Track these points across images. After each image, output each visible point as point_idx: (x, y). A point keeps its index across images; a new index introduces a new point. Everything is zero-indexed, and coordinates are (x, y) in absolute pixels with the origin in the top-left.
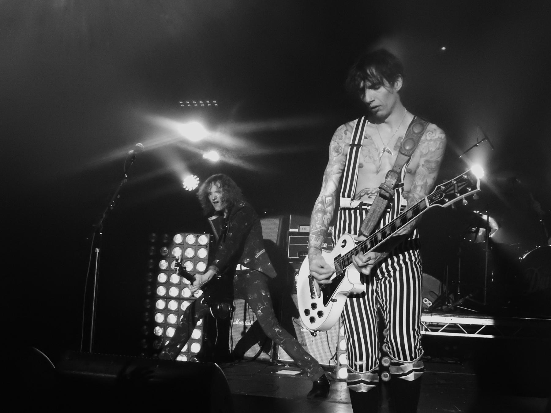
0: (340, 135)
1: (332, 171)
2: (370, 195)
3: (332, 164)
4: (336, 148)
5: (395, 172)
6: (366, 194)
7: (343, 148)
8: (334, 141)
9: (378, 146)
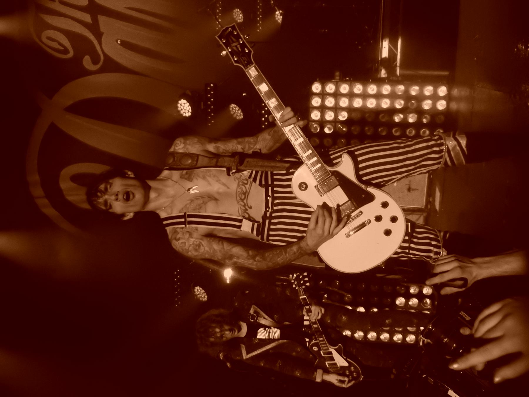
0: (181, 245)
2: (247, 207)
3: (213, 251)
4: (195, 247)
6: (247, 211)
7: (194, 240)
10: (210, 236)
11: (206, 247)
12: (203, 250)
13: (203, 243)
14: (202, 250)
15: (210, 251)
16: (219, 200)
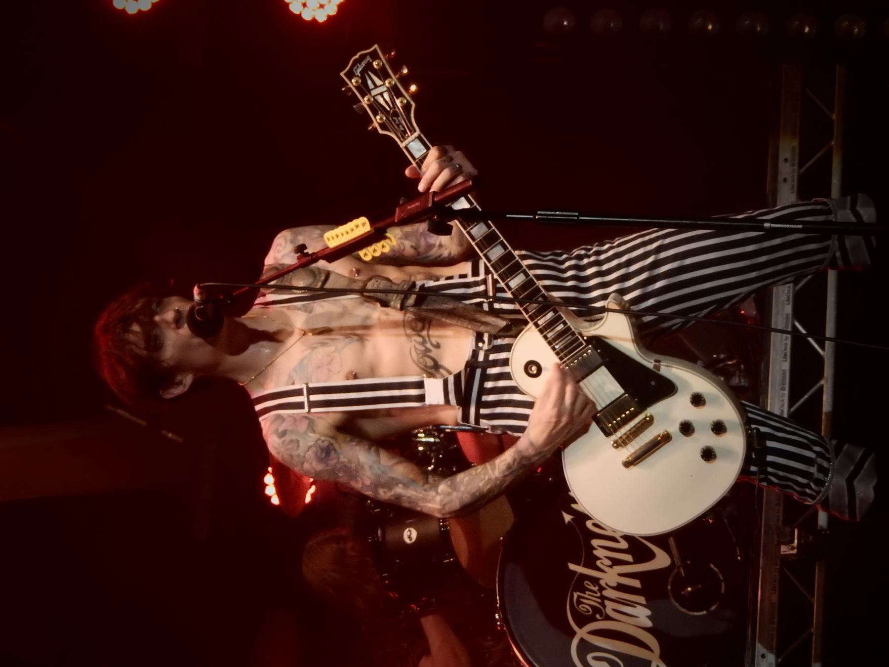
3: (356, 466)
12: (335, 461)
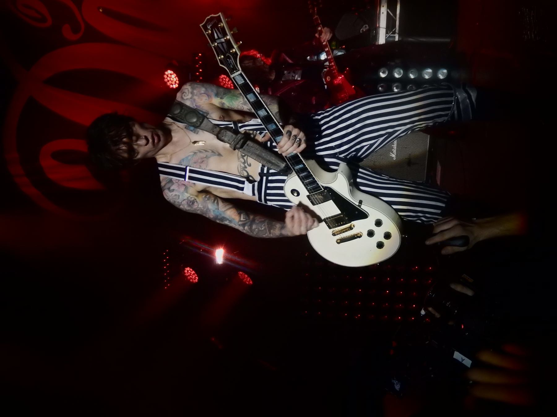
0: (174, 197)
1: (214, 211)
3: (206, 210)
4: (188, 203)
5: (218, 132)
7: (189, 195)
8: (180, 205)
9: (191, 152)
10: (205, 192)
11: (200, 205)
13: (198, 200)
14: (195, 206)
15: (203, 209)
16: (222, 156)
